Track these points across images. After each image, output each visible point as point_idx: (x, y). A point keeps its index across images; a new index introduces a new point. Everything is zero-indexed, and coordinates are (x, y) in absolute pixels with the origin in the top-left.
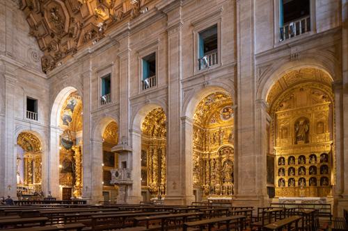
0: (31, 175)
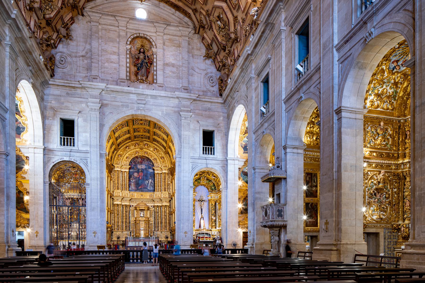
0: (214, 218)
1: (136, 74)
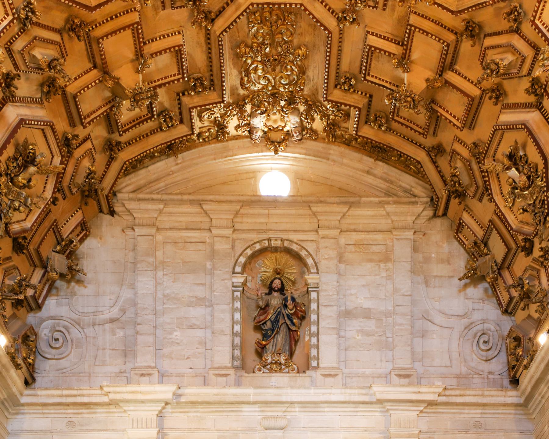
1: (260, 351)
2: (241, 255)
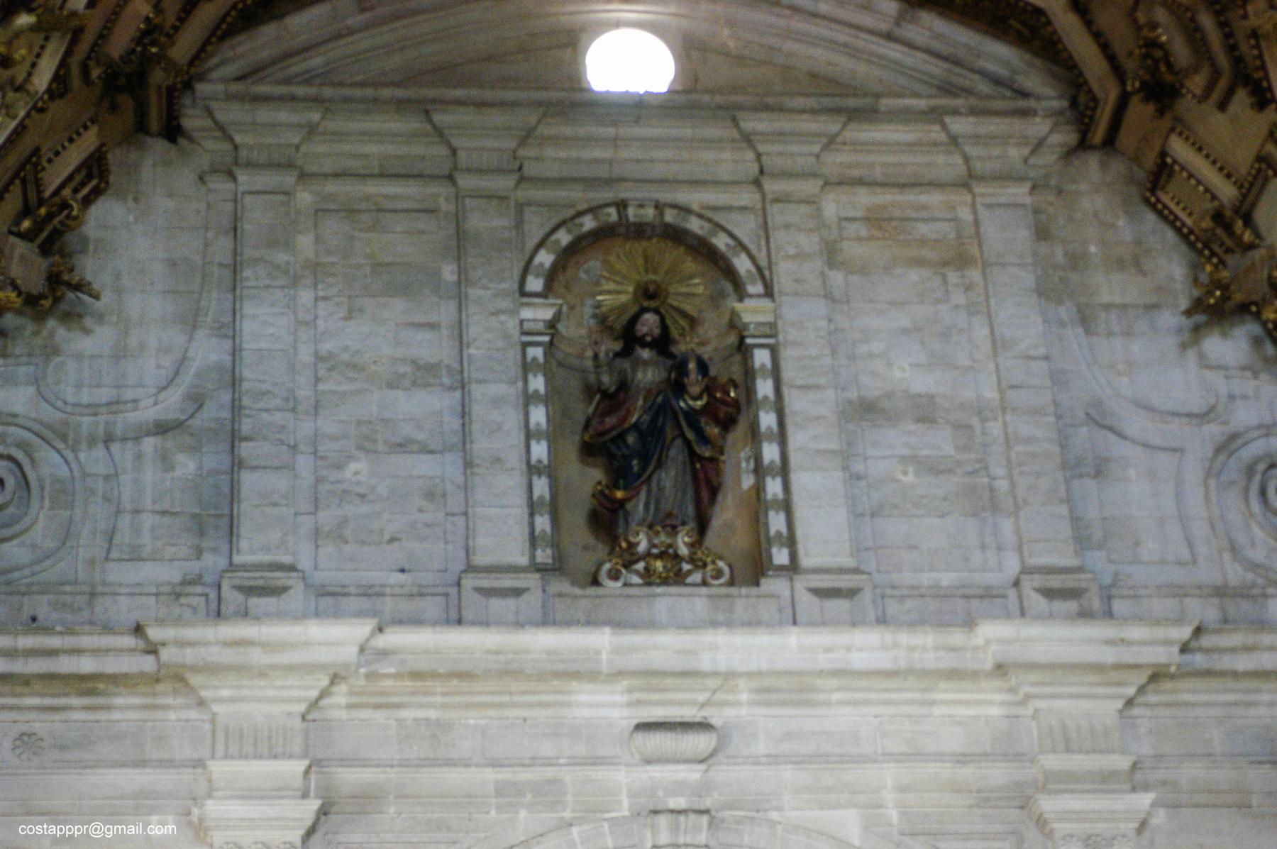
2: (541, 245)
